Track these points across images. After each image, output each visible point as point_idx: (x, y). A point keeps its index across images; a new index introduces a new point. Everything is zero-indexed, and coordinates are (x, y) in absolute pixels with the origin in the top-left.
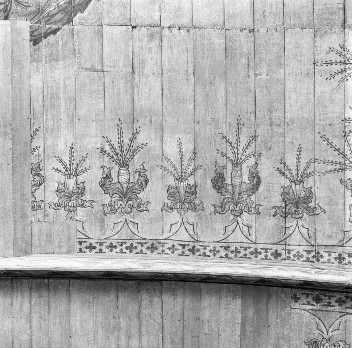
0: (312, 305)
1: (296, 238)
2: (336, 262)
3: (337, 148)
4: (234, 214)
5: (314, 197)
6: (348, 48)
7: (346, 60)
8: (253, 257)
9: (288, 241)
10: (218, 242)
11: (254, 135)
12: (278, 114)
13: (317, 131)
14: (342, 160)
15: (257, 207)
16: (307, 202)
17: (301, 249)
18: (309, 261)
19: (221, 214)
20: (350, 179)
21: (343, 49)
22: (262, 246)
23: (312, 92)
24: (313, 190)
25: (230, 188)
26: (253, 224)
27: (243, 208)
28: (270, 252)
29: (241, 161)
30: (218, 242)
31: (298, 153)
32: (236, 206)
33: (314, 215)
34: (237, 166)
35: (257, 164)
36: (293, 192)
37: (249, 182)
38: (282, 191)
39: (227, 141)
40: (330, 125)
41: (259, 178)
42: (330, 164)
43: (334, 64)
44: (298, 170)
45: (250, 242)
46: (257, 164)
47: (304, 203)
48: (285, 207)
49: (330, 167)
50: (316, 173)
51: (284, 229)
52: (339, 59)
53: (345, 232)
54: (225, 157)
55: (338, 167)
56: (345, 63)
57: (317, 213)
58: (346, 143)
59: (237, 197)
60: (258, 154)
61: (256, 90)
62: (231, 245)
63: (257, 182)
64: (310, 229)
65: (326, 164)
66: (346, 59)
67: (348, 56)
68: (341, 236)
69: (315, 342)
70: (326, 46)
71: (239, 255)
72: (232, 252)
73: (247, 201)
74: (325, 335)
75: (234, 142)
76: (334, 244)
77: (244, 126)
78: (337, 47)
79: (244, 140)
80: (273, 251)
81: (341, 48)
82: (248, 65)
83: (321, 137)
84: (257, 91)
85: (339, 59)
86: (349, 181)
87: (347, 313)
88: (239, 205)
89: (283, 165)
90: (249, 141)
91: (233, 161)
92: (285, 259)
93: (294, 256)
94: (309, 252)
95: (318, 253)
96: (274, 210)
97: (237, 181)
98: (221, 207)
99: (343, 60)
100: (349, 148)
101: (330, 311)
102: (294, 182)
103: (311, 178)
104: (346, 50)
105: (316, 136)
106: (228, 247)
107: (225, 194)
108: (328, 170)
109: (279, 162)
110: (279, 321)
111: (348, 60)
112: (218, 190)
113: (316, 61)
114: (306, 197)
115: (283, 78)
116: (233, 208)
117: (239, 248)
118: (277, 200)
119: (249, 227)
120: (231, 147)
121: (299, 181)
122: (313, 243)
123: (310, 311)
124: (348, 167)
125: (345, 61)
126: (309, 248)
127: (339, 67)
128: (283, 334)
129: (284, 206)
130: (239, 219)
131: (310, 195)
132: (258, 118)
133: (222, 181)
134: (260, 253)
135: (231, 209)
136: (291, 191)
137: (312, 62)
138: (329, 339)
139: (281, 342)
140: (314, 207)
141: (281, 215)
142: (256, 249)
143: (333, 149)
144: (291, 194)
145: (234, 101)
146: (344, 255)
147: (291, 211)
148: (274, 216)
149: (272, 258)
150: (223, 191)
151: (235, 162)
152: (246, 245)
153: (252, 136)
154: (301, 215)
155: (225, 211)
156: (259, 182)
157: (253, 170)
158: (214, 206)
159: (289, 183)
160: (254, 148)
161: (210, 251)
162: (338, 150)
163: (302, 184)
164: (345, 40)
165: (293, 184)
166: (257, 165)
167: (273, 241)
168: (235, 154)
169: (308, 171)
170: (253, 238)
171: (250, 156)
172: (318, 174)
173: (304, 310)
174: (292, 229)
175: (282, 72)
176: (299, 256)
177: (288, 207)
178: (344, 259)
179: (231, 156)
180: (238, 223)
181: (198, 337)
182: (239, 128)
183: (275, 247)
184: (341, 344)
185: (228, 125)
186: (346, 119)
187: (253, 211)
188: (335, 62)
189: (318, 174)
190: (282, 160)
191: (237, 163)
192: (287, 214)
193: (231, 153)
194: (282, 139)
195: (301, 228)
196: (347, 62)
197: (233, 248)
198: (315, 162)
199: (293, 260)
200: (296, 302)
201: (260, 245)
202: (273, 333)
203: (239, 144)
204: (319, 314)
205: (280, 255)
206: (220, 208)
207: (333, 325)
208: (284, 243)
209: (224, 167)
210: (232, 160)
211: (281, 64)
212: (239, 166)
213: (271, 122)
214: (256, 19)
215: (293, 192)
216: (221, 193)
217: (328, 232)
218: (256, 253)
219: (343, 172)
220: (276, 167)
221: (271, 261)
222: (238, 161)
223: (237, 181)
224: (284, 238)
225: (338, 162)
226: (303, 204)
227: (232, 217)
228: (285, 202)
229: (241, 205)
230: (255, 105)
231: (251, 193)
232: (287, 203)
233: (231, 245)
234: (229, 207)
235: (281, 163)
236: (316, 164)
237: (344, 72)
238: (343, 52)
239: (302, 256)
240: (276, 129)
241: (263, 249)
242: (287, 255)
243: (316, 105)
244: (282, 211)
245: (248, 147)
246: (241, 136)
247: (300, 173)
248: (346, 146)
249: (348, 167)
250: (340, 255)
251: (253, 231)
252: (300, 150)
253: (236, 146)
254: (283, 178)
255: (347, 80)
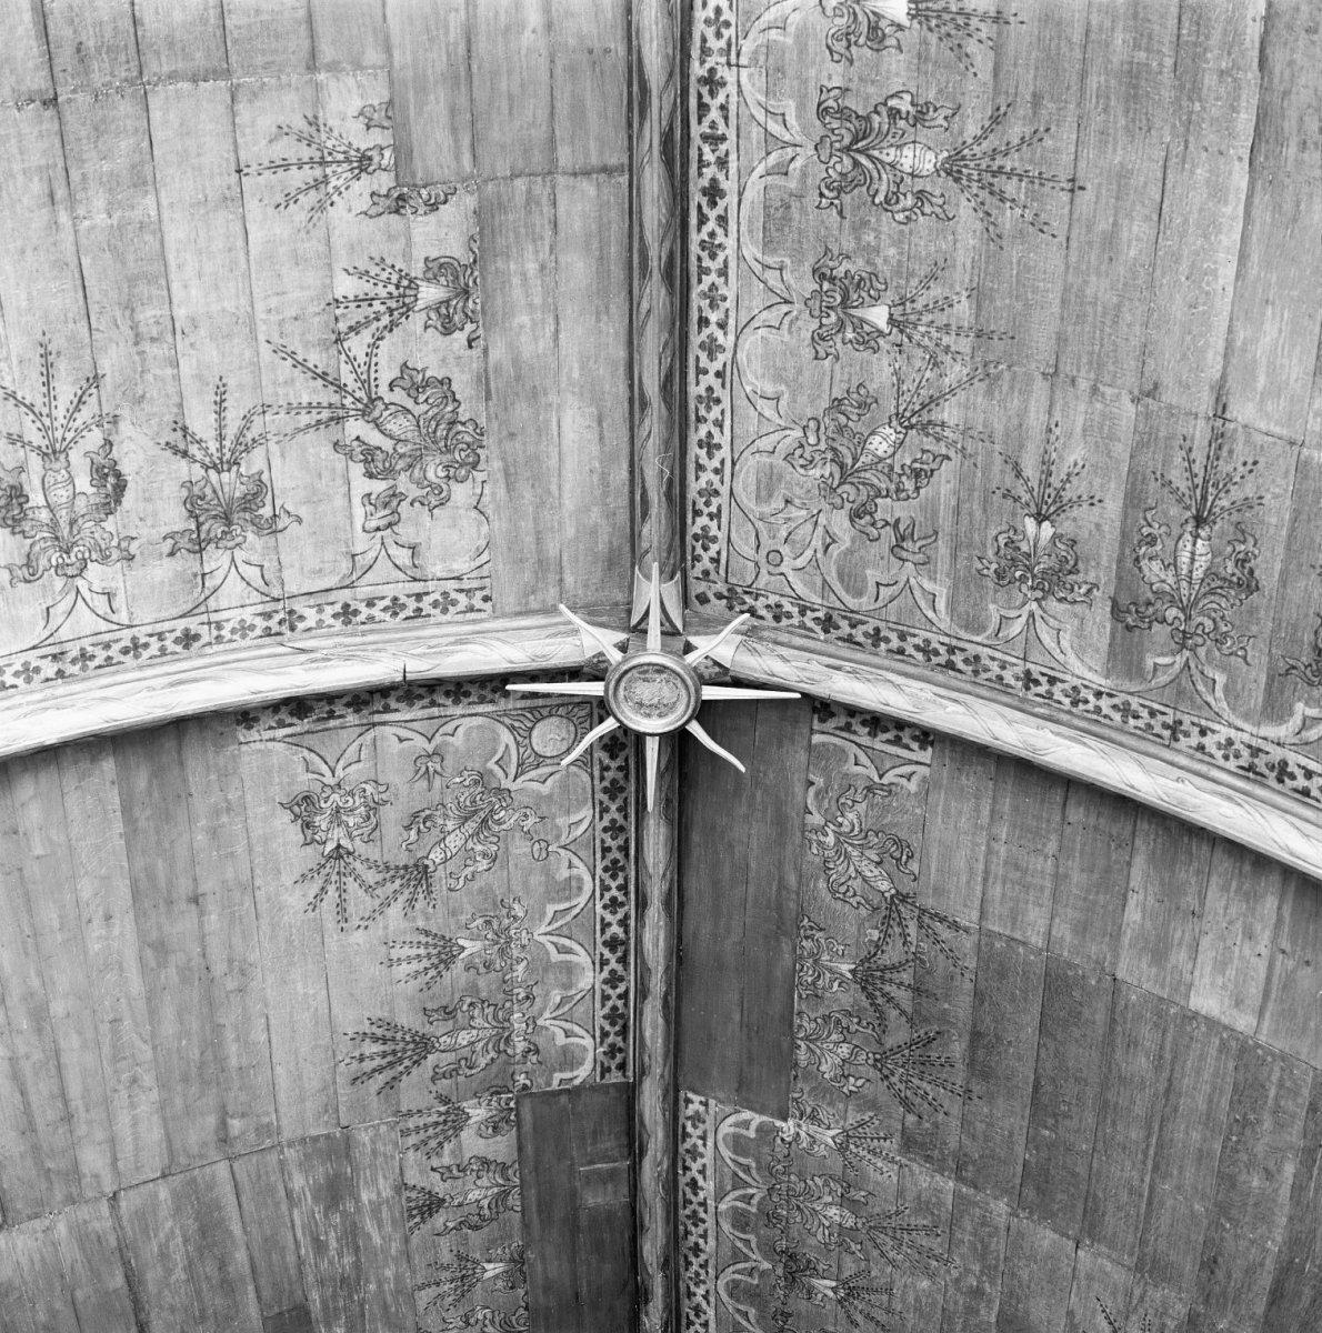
0: (290, 725)
1: (232, 591)
2: (338, 624)
3: (319, 371)
4: (65, 575)
5: (270, 493)
6: (330, 123)
7: (326, 154)
8: (128, 659)
9: (212, 604)
10: (34, 648)
11: (91, 376)
12: (153, 312)
13: (262, 338)
14: (335, 399)
15: (124, 545)
16: (253, 507)
17: (247, 615)
18: (270, 635)
19: (30, 582)
20: (358, 438)
21: (314, 128)
22: (149, 629)
23: (240, 243)
24: (265, 477)
25: (44, 515)
26: (117, 584)
27: (87, 555)
28: (170, 637)
29: (65, 444)
30: (34, 648)
31: (218, 399)
32: (68, 553)
33: (275, 532)
34: (57, 459)
35: (109, 443)
36: (214, 491)
37: (94, 490)
38: (185, 493)
39: (19, 403)
40: (296, 319)
41: (118, 475)
42: (304, 411)
43: (295, 168)
44: (221, 438)
45: (116, 627)
46: (109, 443)
47: (245, 510)
48: (198, 528)
49: (304, 419)
50: (269, 436)
51: (199, 577)
52: (306, 153)
53: (353, 556)
54: (19, 444)
55: (325, 414)
56: (323, 163)
57: (280, 527)
58: (343, 357)
59: (66, 532)
60: (111, 419)
61: (83, 258)
62: (67, 646)
63: (115, 487)
64: (266, 565)
65: (293, 412)
66: (326, 151)
67: (329, 144)
68: (345, 565)
69: (306, 798)
70: (267, 123)
71: (92, 664)
72: (74, 662)
73: (96, 535)
74: (329, 780)
75: (39, 401)
76: (328, 587)
77: (62, 358)
78: (299, 124)
79: (66, 392)
80: (178, 634)
81: (311, 124)
82: (52, 196)
83: (275, 351)
84: (86, 262)
85: (306, 153)
86: (356, 443)
87: (374, 725)
88: (76, 549)
89: (180, 433)
90: (80, 392)
91: (44, 449)
92: (210, 644)
93: (233, 631)
94: (267, 616)
95: (291, 612)
96: (170, 542)
97: (61, 495)
98: (28, 565)
99: (319, 154)
100: (350, 366)
101: (335, 728)
102: (215, 467)
103: (258, 453)
104: (322, 128)
105: (262, 350)
106: (62, 653)
107: (33, 533)
108: (302, 425)
109: (169, 429)
110: (213, 777)
111: (330, 154)
112: (13, 527)
113: (242, 166)
114: (249, 497)
115: (154, 218)
116: (60, 561)
117: (89, 649)
118: (174, 517)
119: (109, 596)
120: (32, 417)
121: (228, 462)
122: (276, 593)
123: (290, 740)
124: (352, 413)
125: (322, 158)
126: (269, 608)
127: (310, 174)
128: (227, 801)
129: (193, 527)
130: (79, 582)
131: (258, 490)
132: (98, 330)
133: (21, 505)
134: (146, 645)
135: (54, 563)
136: (208, 491)
137: (233, 167)
138: (339, 785)
139: (225, 819)
140: (271, 514)
141: (189, 551)
142: (134, 639)
143: (310, 374)
144: (209, 498)
145: (23, 296)
146: (354, 605)
147: (212, 535)
148: (172, 554)
149: (179, 648)
150: (26, 526)
151: (50, 451)
152: (107, 637)
153: (88, 380)
154: (240, 539)
155: (40, 573)
156: (120, 487)
157: (100, 460)
158: (9, 568)
159: (203, 472)
160: (96, 406)
161: (16, 674)
162: (324, 376)
163: (235, 468)
164: (317, 102)
165: (212, 473)
166: (111, 445)
167: (175, 612)
168: (44, 429)
169: (249, 436)
170: (123, 618)
171: (87, 427)
172: (276, 439)
173: (273, 740)
174: (219, 575)
175: (150, 201)
176: (244, 629)
177: (205, 528)
178: (356, 612)
179: (36, 438)
180: (78, 591)
181: (20, 870)
182: (48, 366)
183: (181, 625)
184: (367, 787)
185: (15, 361)
186: (337, 301)
187: (115, 554)
188: (295, 161)
189: (276, 439)
190: (176, 422)
191: (54, 452)
192: (203, 545)
193: (35, 430)
194: (169, 371)
195: (243, 568)
196: (329, 159)
197: (75, 653)
198: (264, 412)
199: (231, 641)
200: (249, 728)
201: (143, 629)
202: (201, 805)
203: (53, 404)
204: (309, 740)
205: (197, 637)
206: (25, 569)
207: (346, 755)
208: (203, 609)
209: (21, 469)
210: (39, 448)
211: (145, 183)
212: (62, 457)
213: (137, 335)
214: (57, 69)
215: (214, 491)
216: (23, 532)
217: (314, 564)
218: (135, 647)
219: (340, 426)
220: (163, 442)
221: (176, 657)
222: (58, 445)
223: (61, 495)
224: (203, 597)
225: (325, 404)
226: (241, 514)
227: (59, 583)
228: (197, 517)
229: (81, 548)
230: (85, 297)
231: (103, 516)
232: (201, 519)
233: (67, 646)
234: (49, 560)
235: (175, 430)
236: (268, 417)
237: (323, 186)
238: (315, 134)
239: (252, 627)
240: (153, 350)
241: (151, 635)
242: (215, 633)
243: (253, 276)
244: (190, 540)
245: (81, 407)
246: (56, 385)
247: (227, 443)
248: (343, 365)
249: (352, 413)
250: (346, 606)
251: (119, 602)
252: (222, 389)
253: (45, 411)
254: (184, 463)
255: (332, 205)
